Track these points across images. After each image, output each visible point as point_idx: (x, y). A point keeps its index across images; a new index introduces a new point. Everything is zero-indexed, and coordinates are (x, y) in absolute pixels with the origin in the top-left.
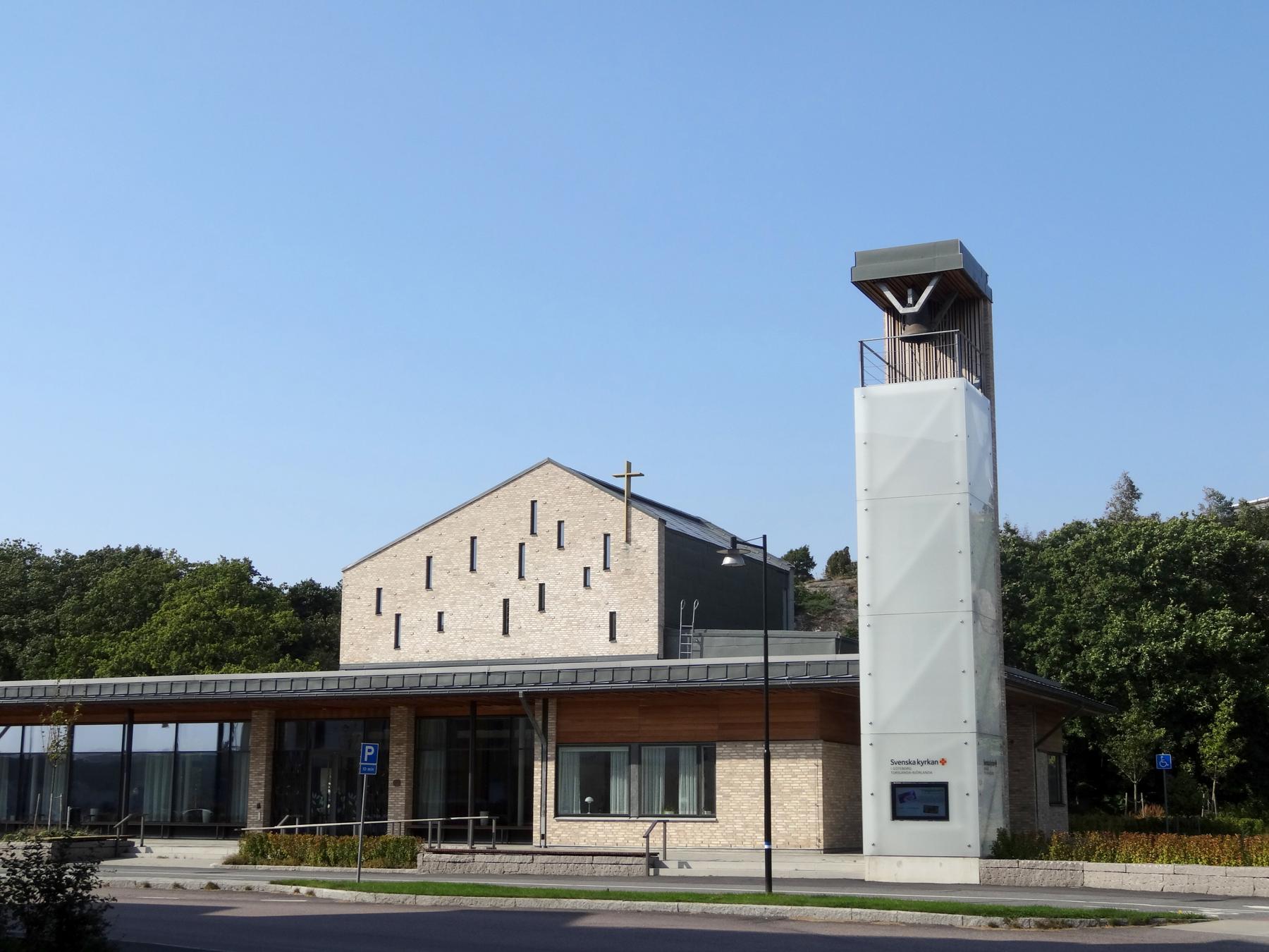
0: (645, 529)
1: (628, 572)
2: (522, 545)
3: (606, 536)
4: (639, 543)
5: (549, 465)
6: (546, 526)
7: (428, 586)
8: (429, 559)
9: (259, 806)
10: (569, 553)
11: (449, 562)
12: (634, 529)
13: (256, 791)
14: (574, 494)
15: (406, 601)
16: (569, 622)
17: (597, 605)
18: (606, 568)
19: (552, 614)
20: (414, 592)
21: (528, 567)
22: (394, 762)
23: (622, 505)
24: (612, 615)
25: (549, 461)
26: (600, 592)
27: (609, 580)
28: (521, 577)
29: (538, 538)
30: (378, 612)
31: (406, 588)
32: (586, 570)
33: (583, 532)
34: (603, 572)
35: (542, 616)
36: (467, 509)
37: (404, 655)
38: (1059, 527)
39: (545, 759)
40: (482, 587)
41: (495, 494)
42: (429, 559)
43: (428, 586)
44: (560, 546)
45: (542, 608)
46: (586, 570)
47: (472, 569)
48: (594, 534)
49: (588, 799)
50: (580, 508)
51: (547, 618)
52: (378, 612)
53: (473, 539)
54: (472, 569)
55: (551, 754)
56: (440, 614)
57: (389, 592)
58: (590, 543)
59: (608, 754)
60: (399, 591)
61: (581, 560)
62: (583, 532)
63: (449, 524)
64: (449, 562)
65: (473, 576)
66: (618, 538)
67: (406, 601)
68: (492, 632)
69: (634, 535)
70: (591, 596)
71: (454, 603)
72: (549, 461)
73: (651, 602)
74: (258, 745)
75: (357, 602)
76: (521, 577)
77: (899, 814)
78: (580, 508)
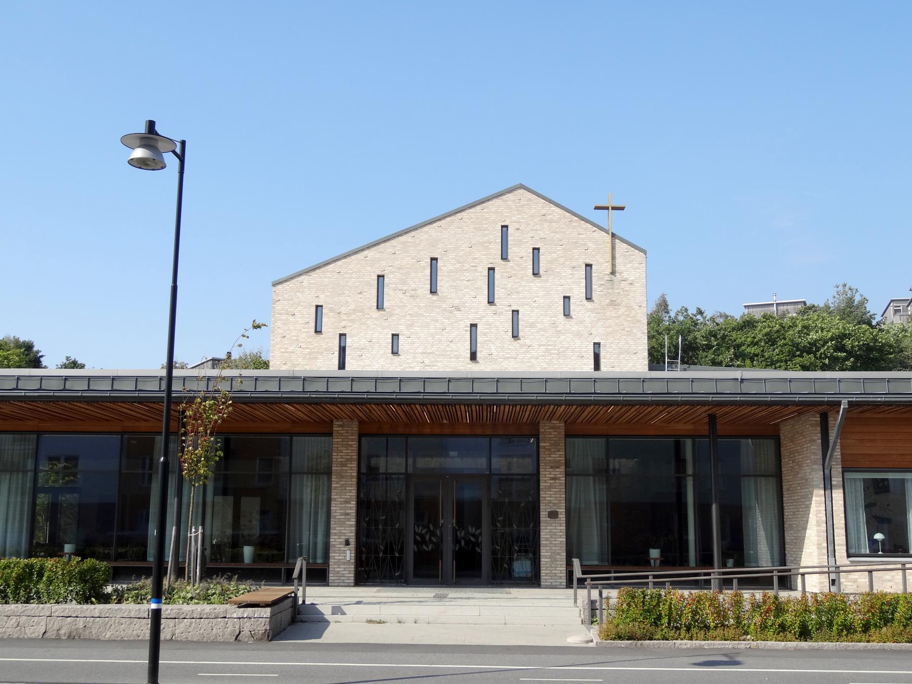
0: (631, 262)
1: (613, 303)
2: (491, 270)
3: (589, 266)
4: (625, 275)
5: (522, 191)
6: (520, 251)
7: (380, 306)
8: (380, 277)
9: (347, 543)
10: (547, 281)
11: (404, 282)
12: (618, 261)
13: (342, 523)
14: (551, 221)
15: (352, 321)
16: (547, 351)
17: (579, 335)
18: (589, 298)
19: (528, 342)
20: (362, 311)
21: (499, 292)
22: (550, 488)
23: (608, 238)
24: (597, 345)
25: (522, 187)
26: (582, 322)
27: (592, 311)
28: (491, 302)
29: (510, 264)
30: (318, 331)
31: (352, 307)
32: (567, 298)
33: (562, 260)
34: (585, 302)
35: (516, 344)
36: (425, 229)
37: (485, 367)
38: (737, 313)
39: (828, 486)
40: (445, 310)
41: (459, 216)
42: (380, 277)
43: (380, 306)
44: (536, 274)
45: (515, 336)
46: (567, 298)
47: (433, 291)
48: (574, 264)
49: (879, 536)
50: (558, 236)
51: (522, 346)
52: (318, 331)
53: (434, 260)
54: (433, 291)
55: (837, 480)
56: (395, 336)
57: (331, 310)
58: (570, 271)
59: (903, 481)
60: (343, 310)
61: (560, 288)
62: (562, 260)
63: (404, 243)
64: (404, 282)
65: (434, 298)
66: (601, 269)
67: (352, 321)
68: (457, 357)
69: (619, 268)
70: (571, 325)
71: (411, 325)
72: (522, 187)
73: (639, 335)
74: (343, 465)
75: (291, 318)
76: (491, 302)
77: (852, 551)
78: (558, 236)
